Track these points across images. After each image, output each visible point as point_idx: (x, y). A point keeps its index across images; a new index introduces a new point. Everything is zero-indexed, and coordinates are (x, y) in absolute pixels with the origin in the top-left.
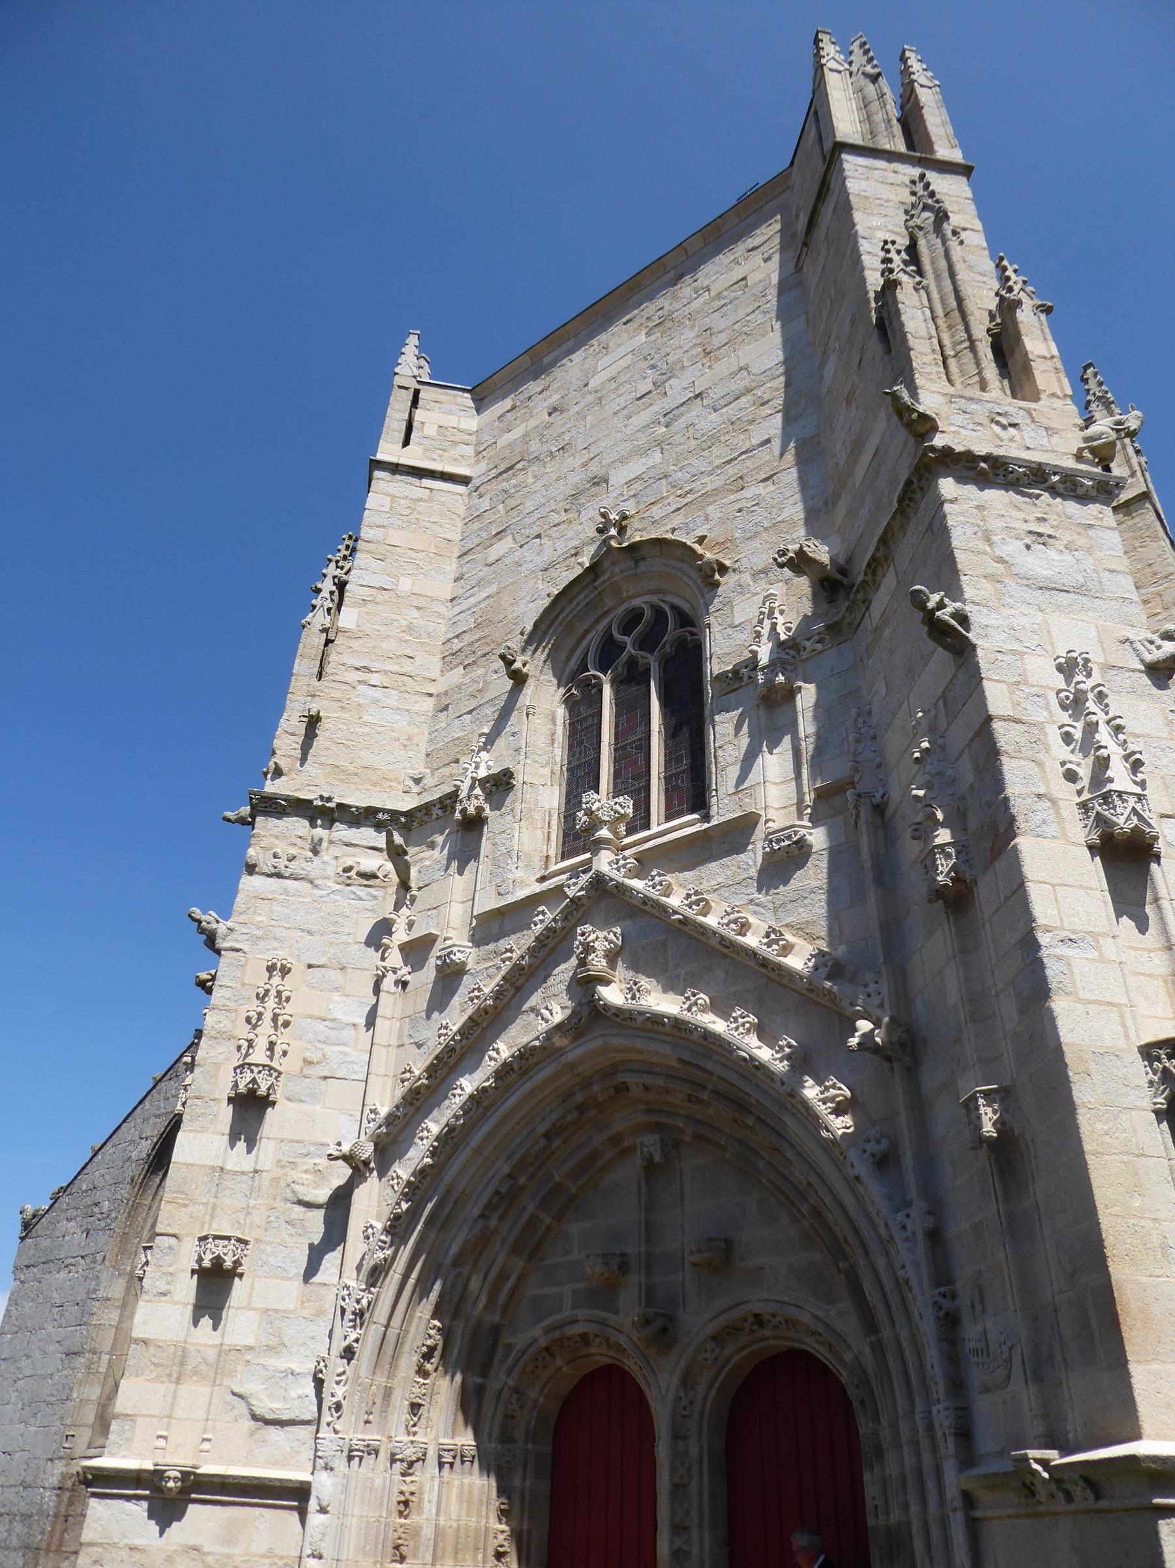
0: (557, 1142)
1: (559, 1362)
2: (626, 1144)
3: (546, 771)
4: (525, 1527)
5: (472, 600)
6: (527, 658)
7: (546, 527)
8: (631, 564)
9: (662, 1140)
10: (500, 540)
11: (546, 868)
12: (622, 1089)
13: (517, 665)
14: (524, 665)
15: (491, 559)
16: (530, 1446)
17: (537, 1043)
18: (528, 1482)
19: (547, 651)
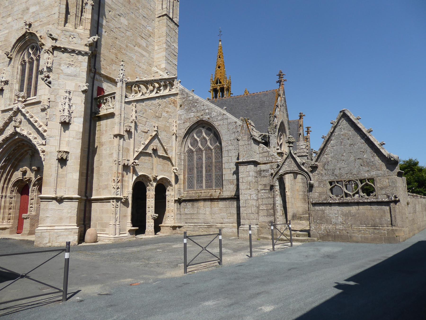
0: (15, 151)
1: (19, 183)
2: (27, 152)
3: (15, 81)
4: (15, 205)
5: (4, 32)
6: (12, 54)
7: (18, 18)
8: (31, 36)
9: (32, 152)
10: (10, 17)
11: (15, 102)
12: (24, 144)
13: (9, 56)
14: (11, 55)
15: (8, 22)
16: (15, 194)
17: (8, 136)
18: (15, 199)
19: (16, 52)
